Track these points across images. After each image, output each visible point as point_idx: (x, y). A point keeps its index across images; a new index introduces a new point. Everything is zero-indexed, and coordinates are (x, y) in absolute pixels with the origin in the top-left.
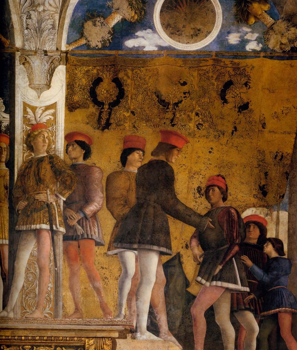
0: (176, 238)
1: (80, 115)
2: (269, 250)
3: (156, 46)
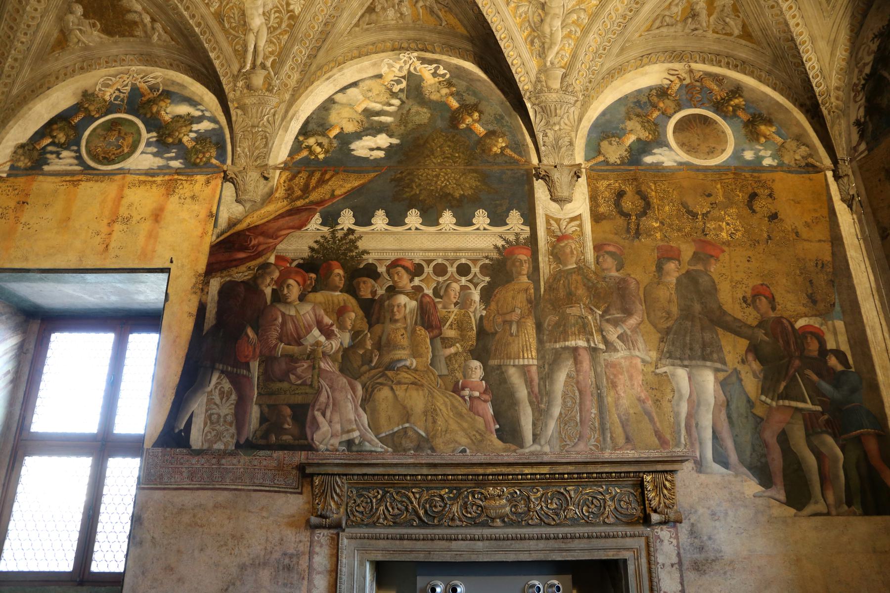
0: (729, 352)
1: (606, 225)
2: (833, 361)
3: (675, 161)
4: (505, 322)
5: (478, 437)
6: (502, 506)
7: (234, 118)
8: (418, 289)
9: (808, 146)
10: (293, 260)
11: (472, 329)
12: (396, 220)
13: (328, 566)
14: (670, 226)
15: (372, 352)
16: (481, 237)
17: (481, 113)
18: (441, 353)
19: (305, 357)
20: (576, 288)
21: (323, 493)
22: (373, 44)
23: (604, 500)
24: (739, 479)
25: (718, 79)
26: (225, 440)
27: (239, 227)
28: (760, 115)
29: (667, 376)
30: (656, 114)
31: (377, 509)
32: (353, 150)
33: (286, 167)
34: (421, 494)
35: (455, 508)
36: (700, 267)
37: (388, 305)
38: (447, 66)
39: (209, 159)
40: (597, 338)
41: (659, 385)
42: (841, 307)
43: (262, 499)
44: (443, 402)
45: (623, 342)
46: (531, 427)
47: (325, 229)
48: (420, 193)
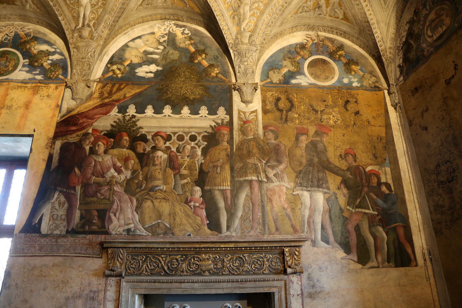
1: (270, 116)
3: (308, 83)
4: (214, 166)
5: (198, 228)
6: (210, 264)
7: (72, 54)
8: (168, 148)
9: (376, 77)
10: (102, 131)
11: (196, 170)
12: (158, 111)
13: (115, 298)
14: (304, 116)
15: (142, 182)
16: (203, 121)
17: (206, 54)
18: (179, 182)
19: (106, 184)
20: (253, 149)
21: (113, 258)
22: (150, 16)
23: (263, 261)
24: (334, 250)
25: (332, 41)
26: (60, 229)
27: (73, 113)
28: (352, 60)
29: (299, 196)
30: (299, 58)
31: (142, 266)
32: (137, 73)
33: (100, 81)
34: (166, 258)
35: (184, 266)
36: (318, 139)
37: (152, 157)
38: (190, 29)
39: (58, 75)
40: (263, 175)
41: (295, 201)
42: (389, 160)
43: (80, 261)
44: (180, 209)
45: (276, 177)
46: (226, 222)
47: (120, 115)
48: (172, 96)
